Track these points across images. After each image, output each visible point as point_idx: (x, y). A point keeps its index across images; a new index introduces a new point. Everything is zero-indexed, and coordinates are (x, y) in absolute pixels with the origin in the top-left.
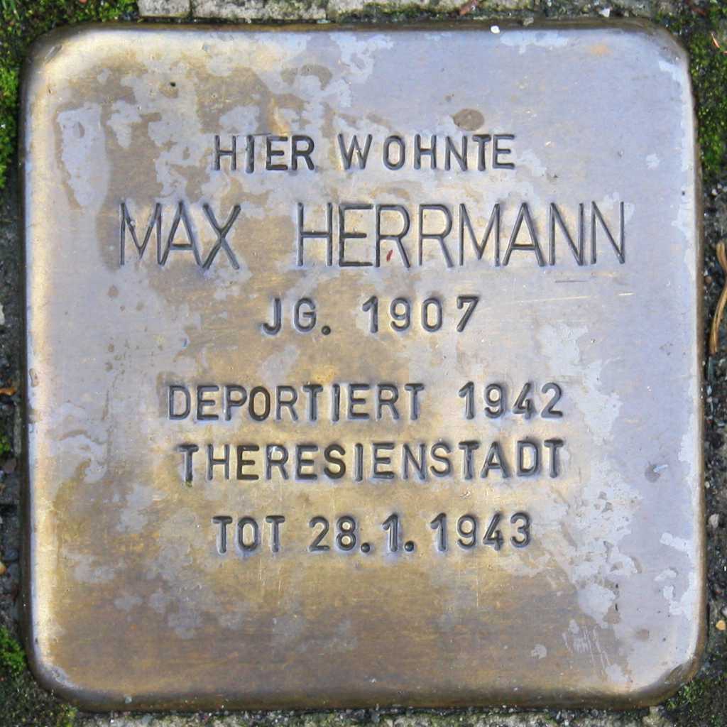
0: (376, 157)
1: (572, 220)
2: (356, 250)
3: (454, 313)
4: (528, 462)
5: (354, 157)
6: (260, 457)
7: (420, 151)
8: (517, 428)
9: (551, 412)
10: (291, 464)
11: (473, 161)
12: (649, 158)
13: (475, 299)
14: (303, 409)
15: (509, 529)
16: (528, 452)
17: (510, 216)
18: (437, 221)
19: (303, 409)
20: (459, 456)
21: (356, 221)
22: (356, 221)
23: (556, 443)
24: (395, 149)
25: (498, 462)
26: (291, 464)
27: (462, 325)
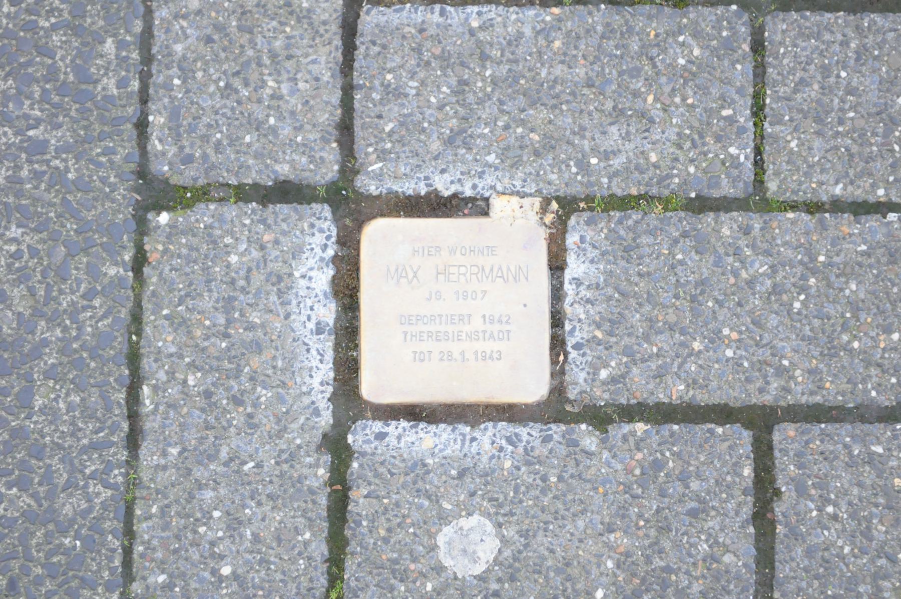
0: (458, 252)
1: (522, 277)
2: (453, 278)
3: (480, 295)
4: (501, 334)
5: (452, 251)
6: (425, 335)
7: (471, 251)
8: (497, 327)
9: (507, 322)
10: (434, 337)
11: (485, 252)
12: (675, 319)
13: (485, 291)
14: (437, 321)
15: (495, 355)
16: (501, 334)
17: (495, 270)
18: (475, 270)
19: (437, 321)
20: (481, 335)
21: (452, 270)
22: (452, 270)
23: (508, 331)
24: (463, 250)
25: (492, 336)
26: (434, 337)
27: (482, 299)
